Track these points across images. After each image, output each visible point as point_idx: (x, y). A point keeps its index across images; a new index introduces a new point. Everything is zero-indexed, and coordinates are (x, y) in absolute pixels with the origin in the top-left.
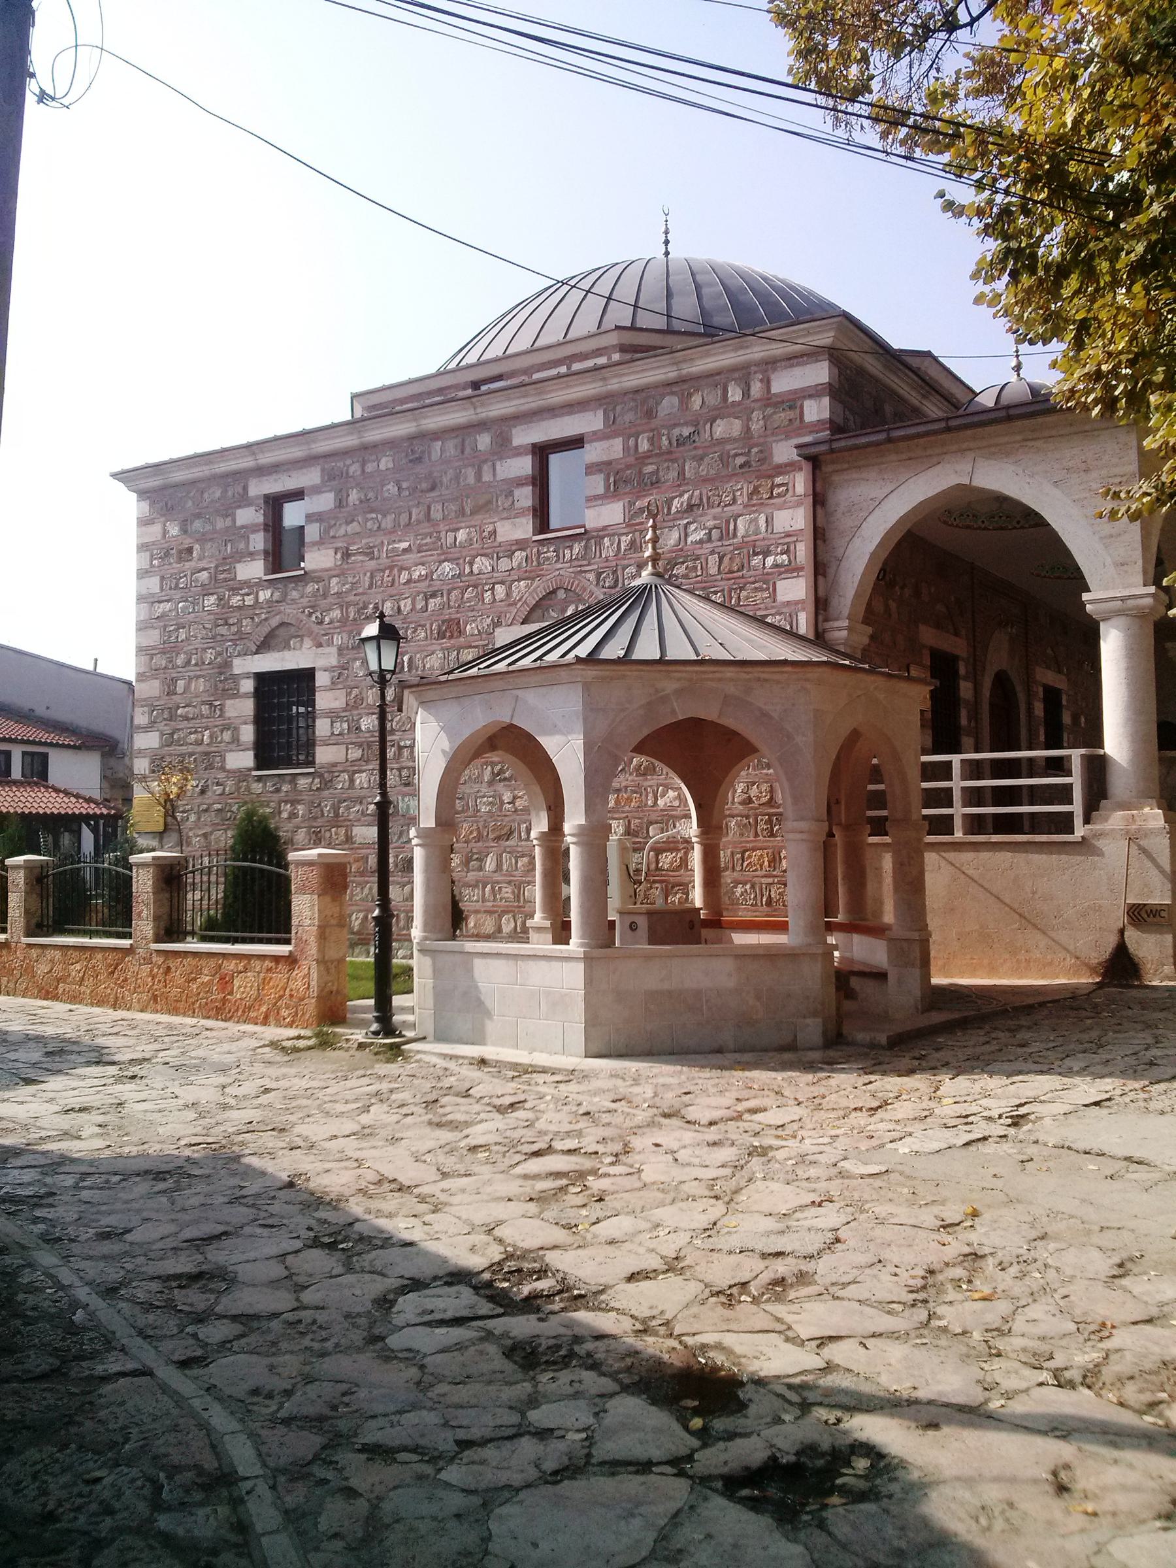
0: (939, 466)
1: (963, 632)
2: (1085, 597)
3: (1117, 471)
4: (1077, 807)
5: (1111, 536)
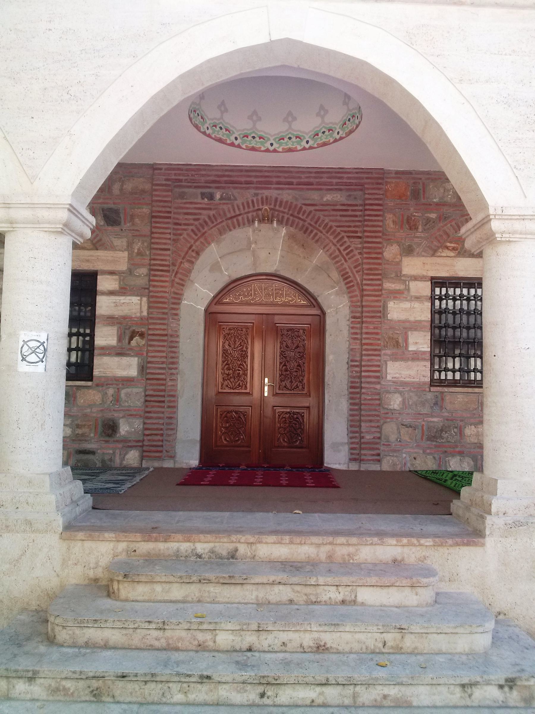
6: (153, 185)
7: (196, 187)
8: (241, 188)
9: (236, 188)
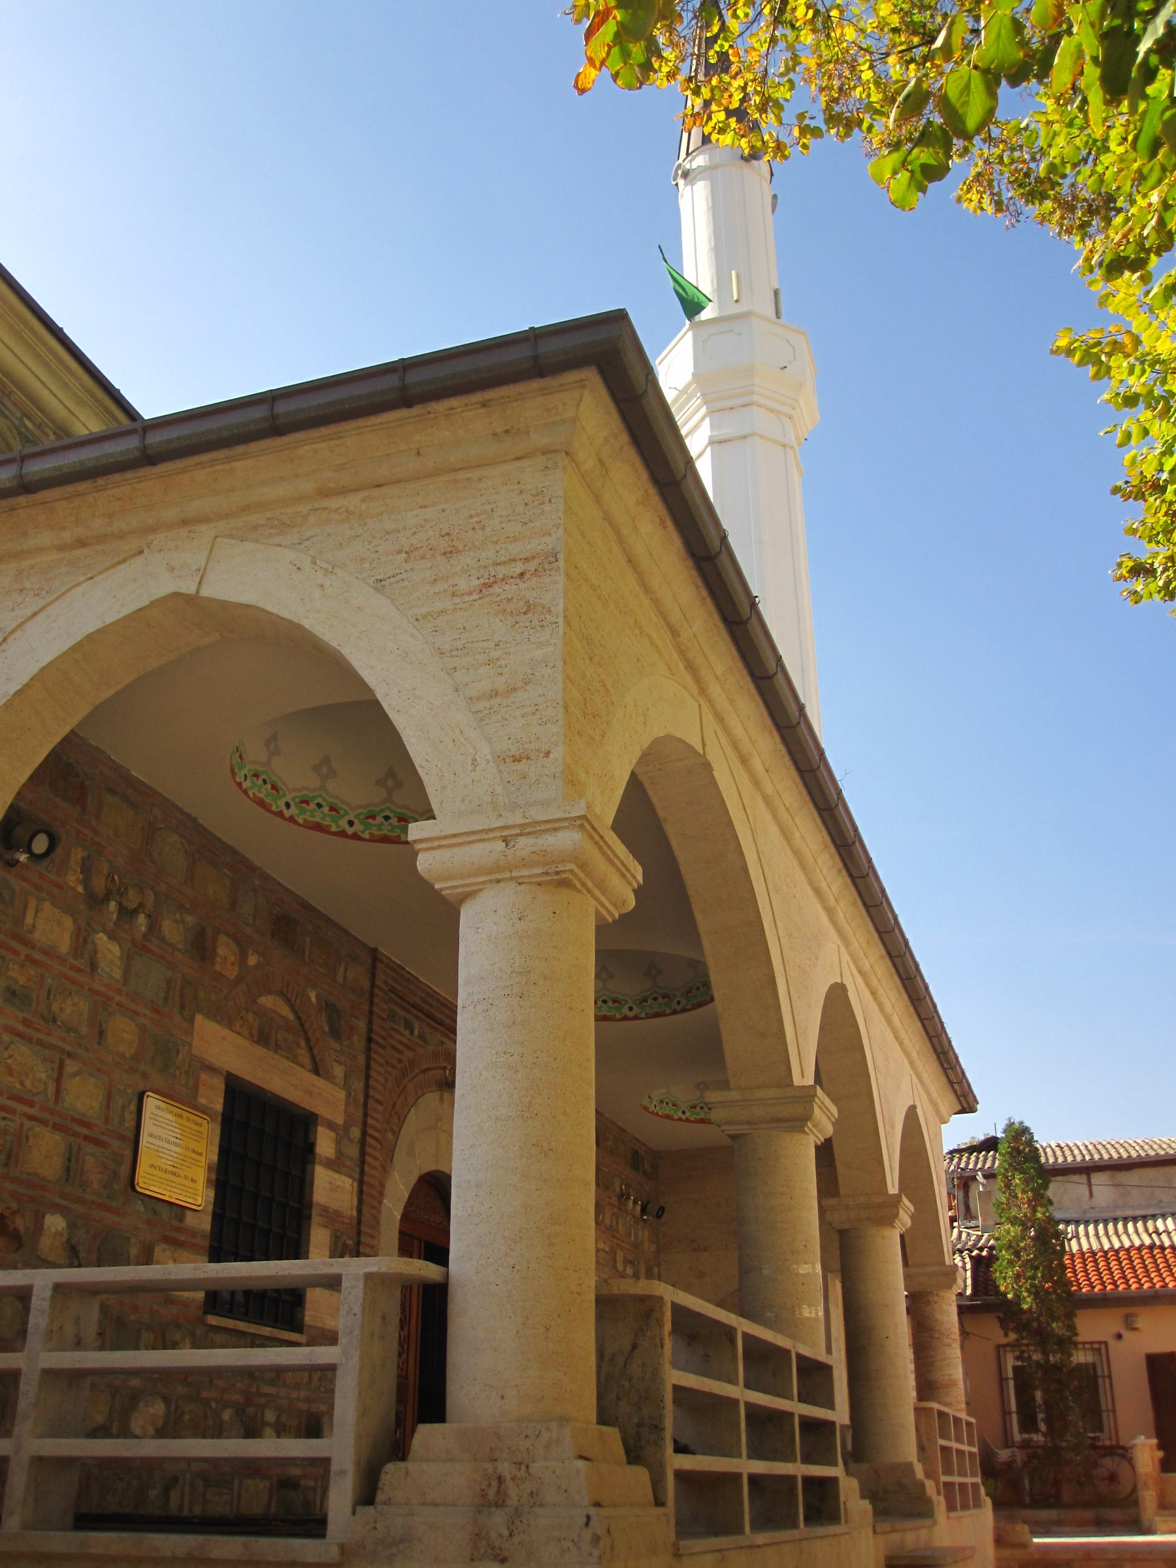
0: (139, 561)
1: (339, 1071)
2: (416, 831)
3: (515, 549)
4: (341, 1447)
5: (495, 694)
6: (373, 985)
7: (401, 1007)
8: (432, 1027)
9: (428, 1024)
